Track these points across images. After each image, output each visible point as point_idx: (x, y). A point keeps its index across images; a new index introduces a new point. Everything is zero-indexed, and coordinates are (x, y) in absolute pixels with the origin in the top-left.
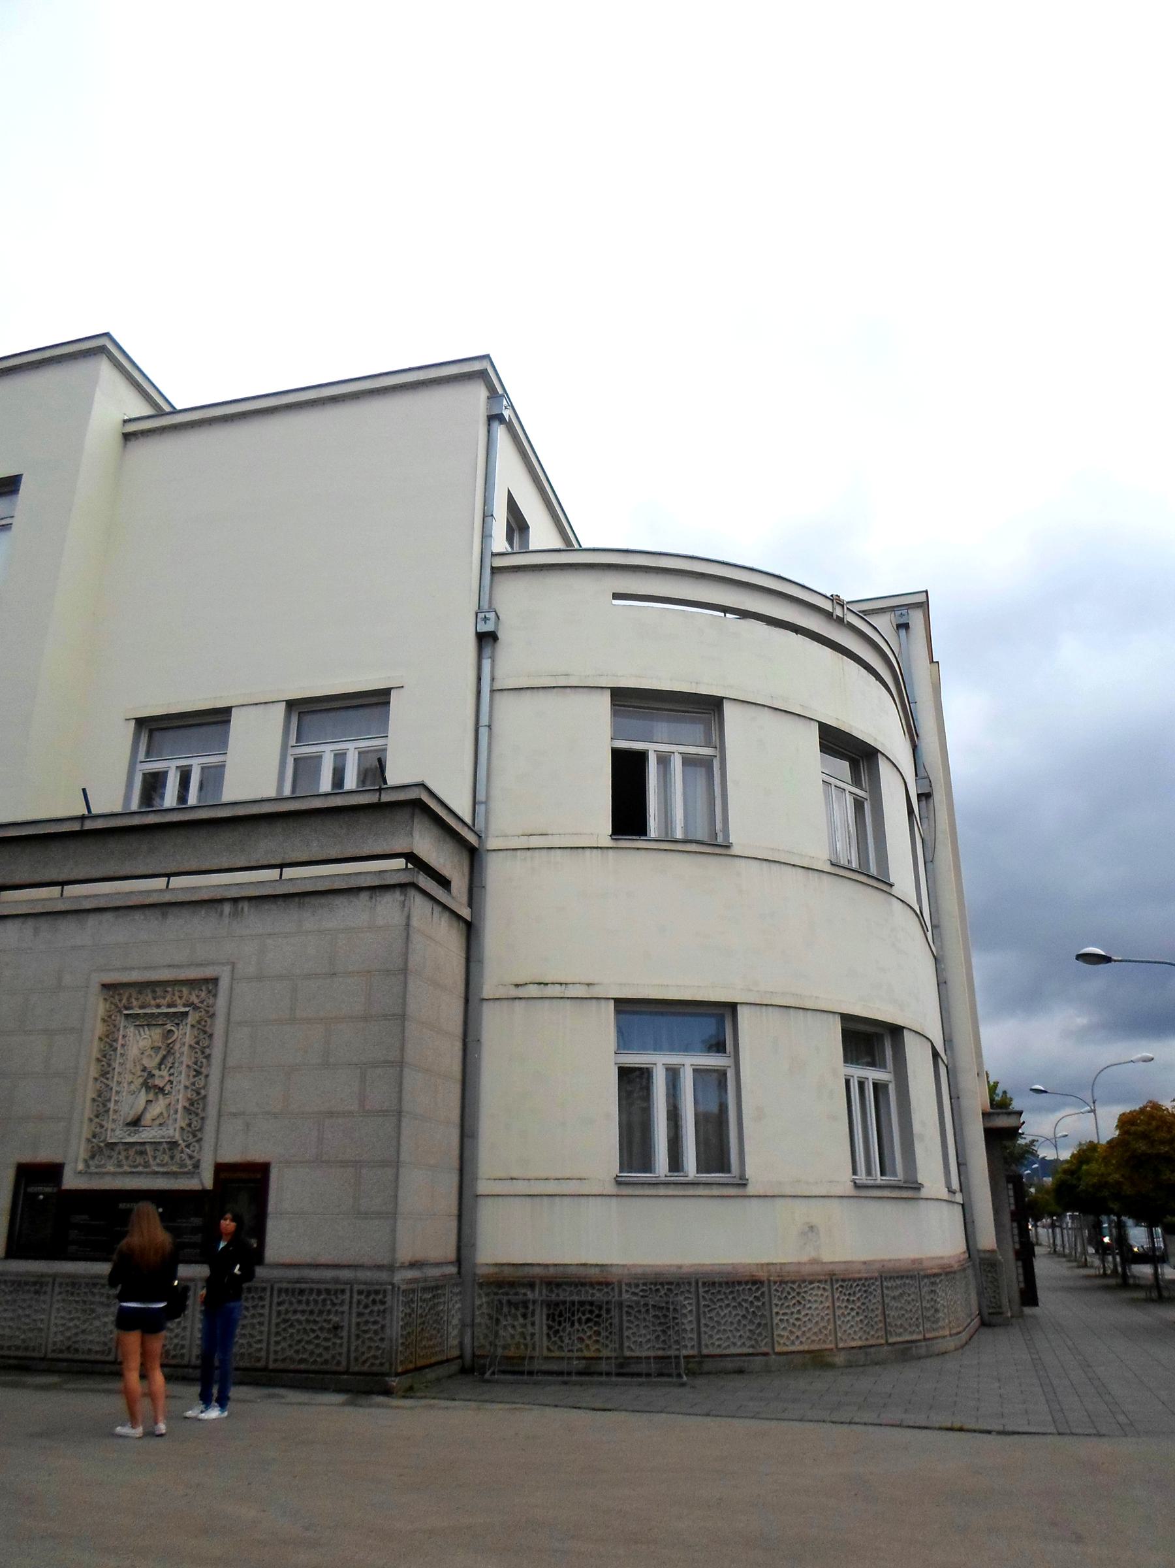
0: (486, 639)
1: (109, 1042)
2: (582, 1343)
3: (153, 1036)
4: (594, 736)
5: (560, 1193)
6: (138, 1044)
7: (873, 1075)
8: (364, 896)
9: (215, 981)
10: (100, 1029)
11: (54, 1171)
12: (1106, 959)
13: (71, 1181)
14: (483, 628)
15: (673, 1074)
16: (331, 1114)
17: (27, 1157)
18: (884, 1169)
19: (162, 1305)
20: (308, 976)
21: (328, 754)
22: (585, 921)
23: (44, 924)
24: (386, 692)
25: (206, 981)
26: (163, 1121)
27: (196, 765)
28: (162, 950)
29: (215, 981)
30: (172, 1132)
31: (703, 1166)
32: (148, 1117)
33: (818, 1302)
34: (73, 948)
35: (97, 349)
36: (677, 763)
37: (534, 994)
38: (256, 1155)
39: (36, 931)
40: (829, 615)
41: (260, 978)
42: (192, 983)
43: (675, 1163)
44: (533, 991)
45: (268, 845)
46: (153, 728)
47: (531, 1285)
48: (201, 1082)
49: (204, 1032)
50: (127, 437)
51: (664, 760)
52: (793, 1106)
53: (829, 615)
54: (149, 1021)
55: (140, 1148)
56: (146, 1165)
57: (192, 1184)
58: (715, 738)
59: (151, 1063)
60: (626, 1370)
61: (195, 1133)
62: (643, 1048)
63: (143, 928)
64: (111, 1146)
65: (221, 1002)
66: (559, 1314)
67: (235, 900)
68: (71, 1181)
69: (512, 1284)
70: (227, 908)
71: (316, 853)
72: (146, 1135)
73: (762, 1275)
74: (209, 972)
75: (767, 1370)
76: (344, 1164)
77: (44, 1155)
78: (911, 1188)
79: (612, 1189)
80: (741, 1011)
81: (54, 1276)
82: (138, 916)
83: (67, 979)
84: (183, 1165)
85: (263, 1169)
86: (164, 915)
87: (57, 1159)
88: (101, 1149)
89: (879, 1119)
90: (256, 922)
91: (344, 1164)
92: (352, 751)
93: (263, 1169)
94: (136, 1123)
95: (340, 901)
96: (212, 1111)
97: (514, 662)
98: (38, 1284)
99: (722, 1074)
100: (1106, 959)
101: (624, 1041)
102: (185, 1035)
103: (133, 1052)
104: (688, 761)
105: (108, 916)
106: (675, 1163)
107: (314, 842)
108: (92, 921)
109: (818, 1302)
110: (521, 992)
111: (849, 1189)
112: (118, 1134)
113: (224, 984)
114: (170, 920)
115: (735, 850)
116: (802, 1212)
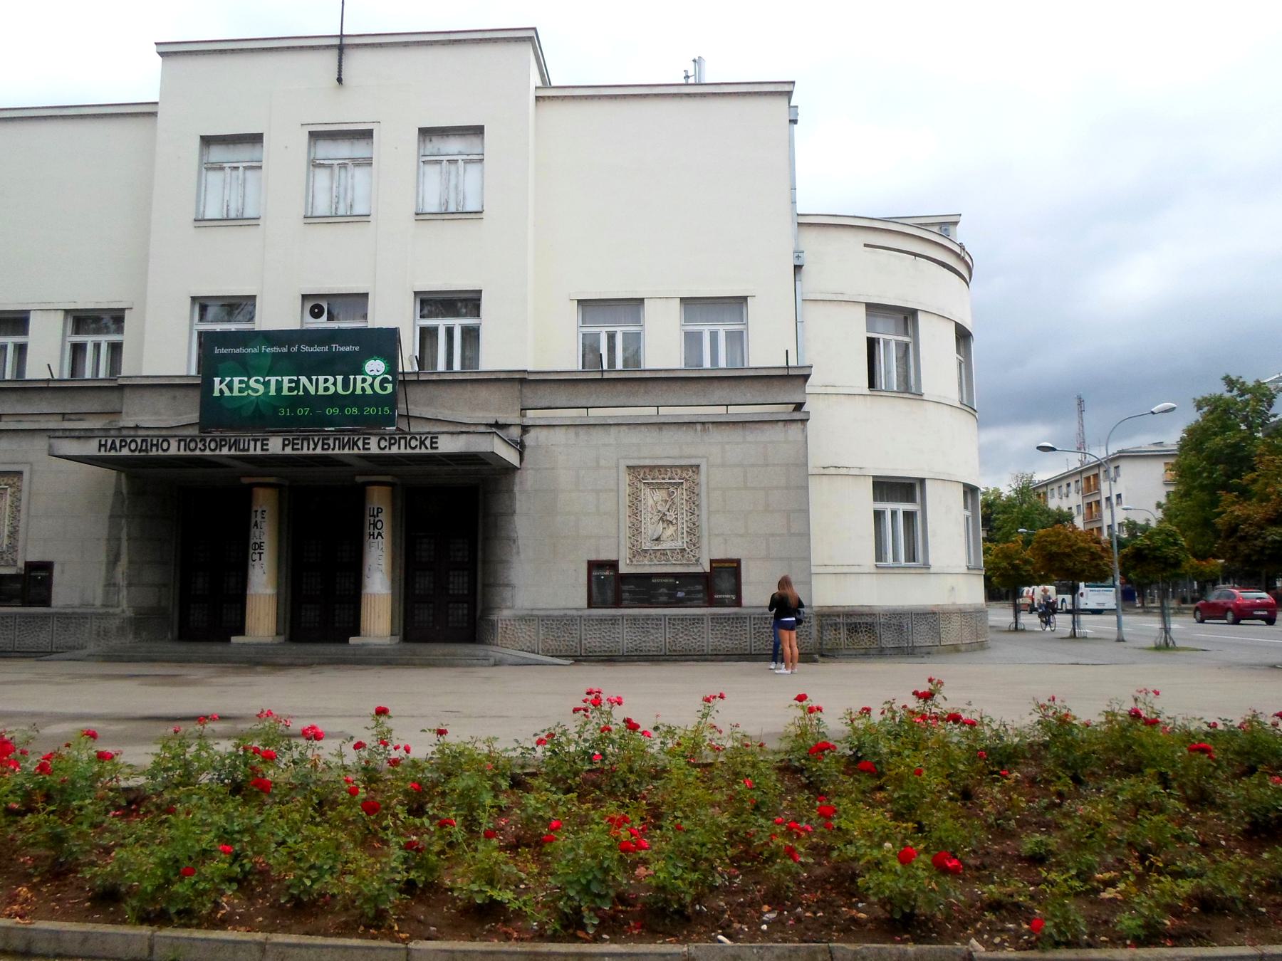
0: (798, 268)
1: (635, 498)
2: (864, 640)
3: (660, 495)
4: (856, 329)
6: (652, 499)
8: (781, 424)
9: (698, 466)
10: (628, 490)
11: (613, 565)
12: (1053, 449)
13: (623, 569)
14: (798, 263)
15: (894, 513)
16: (773, 535)
17: (593, 558)
20: (753, 465)
21: (706, 330)
22: (857, 434)
23: (582, 431)
24: (745, 298)
25: (692, 466)
26: (672, 538)
27: (619, 331)
28: (664, 448)
29: (698, 466)
30: (678, 544)
32: (664, 537)
33: (956, 623)
34: (604, 445)
36: (893, 345)
37: (833, 472)
38: (732, 554)
39: (577, 434)
40: (958, 256)
41: (723, 465)
43: (895, 558)
44: (833, 471)
45: (720, 393)
47: (838, 616)
48: (695, 518)
49: (691, 491)
50: (537, 98)
51: (887, 343)
53: (958, 256)
54: (659, 486)
55: (664, 552)
56: (668, 560)
57: (698, 570)
58: (910, 331)
59: (664, 509)
60: (882, 653)
61: (695, 545)
62: (882, 500)
63: (650, 436)
64: (646, 551)
65: (703, 478)
66: (853, 629)
67: (703, 423)
68: (623, 569)
69: (829, 615)
70: (699, 427)
71: (749, 399)
73: (936, 610)
74: (693, 462)
75: (938, 653)
76: (781, 559)
77: (605, 556)
79: (874, 570)
80: (928, 483)
81: (622, 616)
82: (643, 428)
83: (602, 463)
84: (689, 560)
85: (738, 561)
86: (660, 429)
87: (613, 558)
88: (638, 552)
90: (717, 436)
91: (781, 559)
92: (722, 330)
93: (738, 561)
94: (658, 539)
95: (766, 426)
96: (705, 533)
97: (813, 282)
98: (614, 620)
100: (1053, 449)
101: (875, 499)
102: (681, 495)
103: (651, 502)
104: (897, 343)
105: (624, 428)
106: (895, 558)
107: (747, 393)
108: (613, 430)
109: (956, 623)
110: (826, 471)
111: (965, 570)
112: (647, 545)
113: (703, 469)
114: (664, 432)
115: (925, 397)
116: (951, 581)
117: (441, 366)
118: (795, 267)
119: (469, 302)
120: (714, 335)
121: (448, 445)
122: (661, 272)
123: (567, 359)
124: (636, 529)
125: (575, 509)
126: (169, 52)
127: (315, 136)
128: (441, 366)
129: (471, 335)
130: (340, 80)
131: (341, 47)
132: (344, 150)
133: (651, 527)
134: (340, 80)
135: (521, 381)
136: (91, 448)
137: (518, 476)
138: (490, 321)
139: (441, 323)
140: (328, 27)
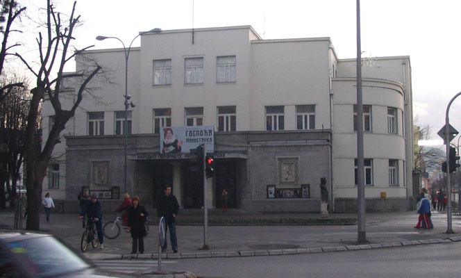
5: (344, 187)
6: (285, 168)
7: (393, 168)
18: (394, 183)
19: (49, 241)
30: (292, 181)
31: (367, 183)
35: (248, 28)
42: (294, 158)
46: (270, 109)
49: (296, 166)
52: (381, 171)
61: (297, 180)
72: (288, 181)
78: (398, 185)
89: (394, 176)
92: (308, 115)
94: (287, 179)
99: (370, 169)
112: (284, 180)
117: (225, 130)
118: (330, 95)
119: (232, 109)
120: (306, 117)
121: (227, 156)
122: (290, 99)
123: (263, 128)
124: (280, 176)
125: (263, 173)
126: (142, 34)
127: (186, 59)
128: (225, 130)
129: (233, 118)
130: (193, 42)
131: (193, 32)
132: (195, 62)
133: (285, 176)
134: (193, 42)
135: (248, 133)
136: (136, 158)
137: (248, 161)
138: (239, 115)
139: (225, 115)
140: (189, 27)
